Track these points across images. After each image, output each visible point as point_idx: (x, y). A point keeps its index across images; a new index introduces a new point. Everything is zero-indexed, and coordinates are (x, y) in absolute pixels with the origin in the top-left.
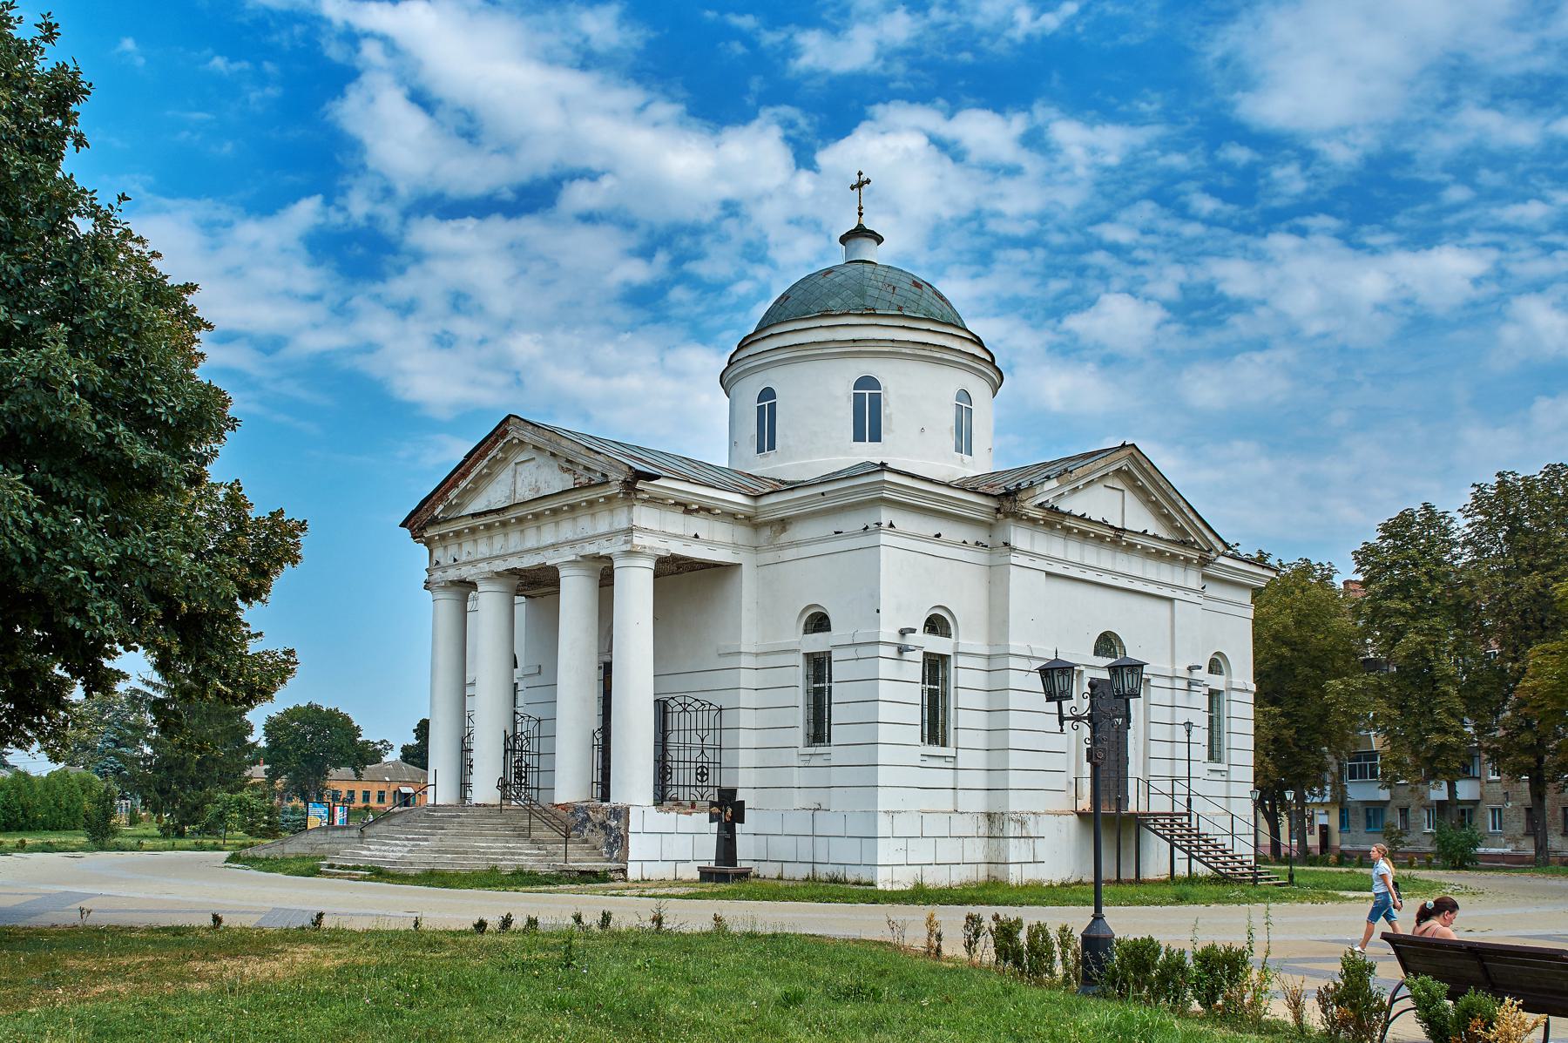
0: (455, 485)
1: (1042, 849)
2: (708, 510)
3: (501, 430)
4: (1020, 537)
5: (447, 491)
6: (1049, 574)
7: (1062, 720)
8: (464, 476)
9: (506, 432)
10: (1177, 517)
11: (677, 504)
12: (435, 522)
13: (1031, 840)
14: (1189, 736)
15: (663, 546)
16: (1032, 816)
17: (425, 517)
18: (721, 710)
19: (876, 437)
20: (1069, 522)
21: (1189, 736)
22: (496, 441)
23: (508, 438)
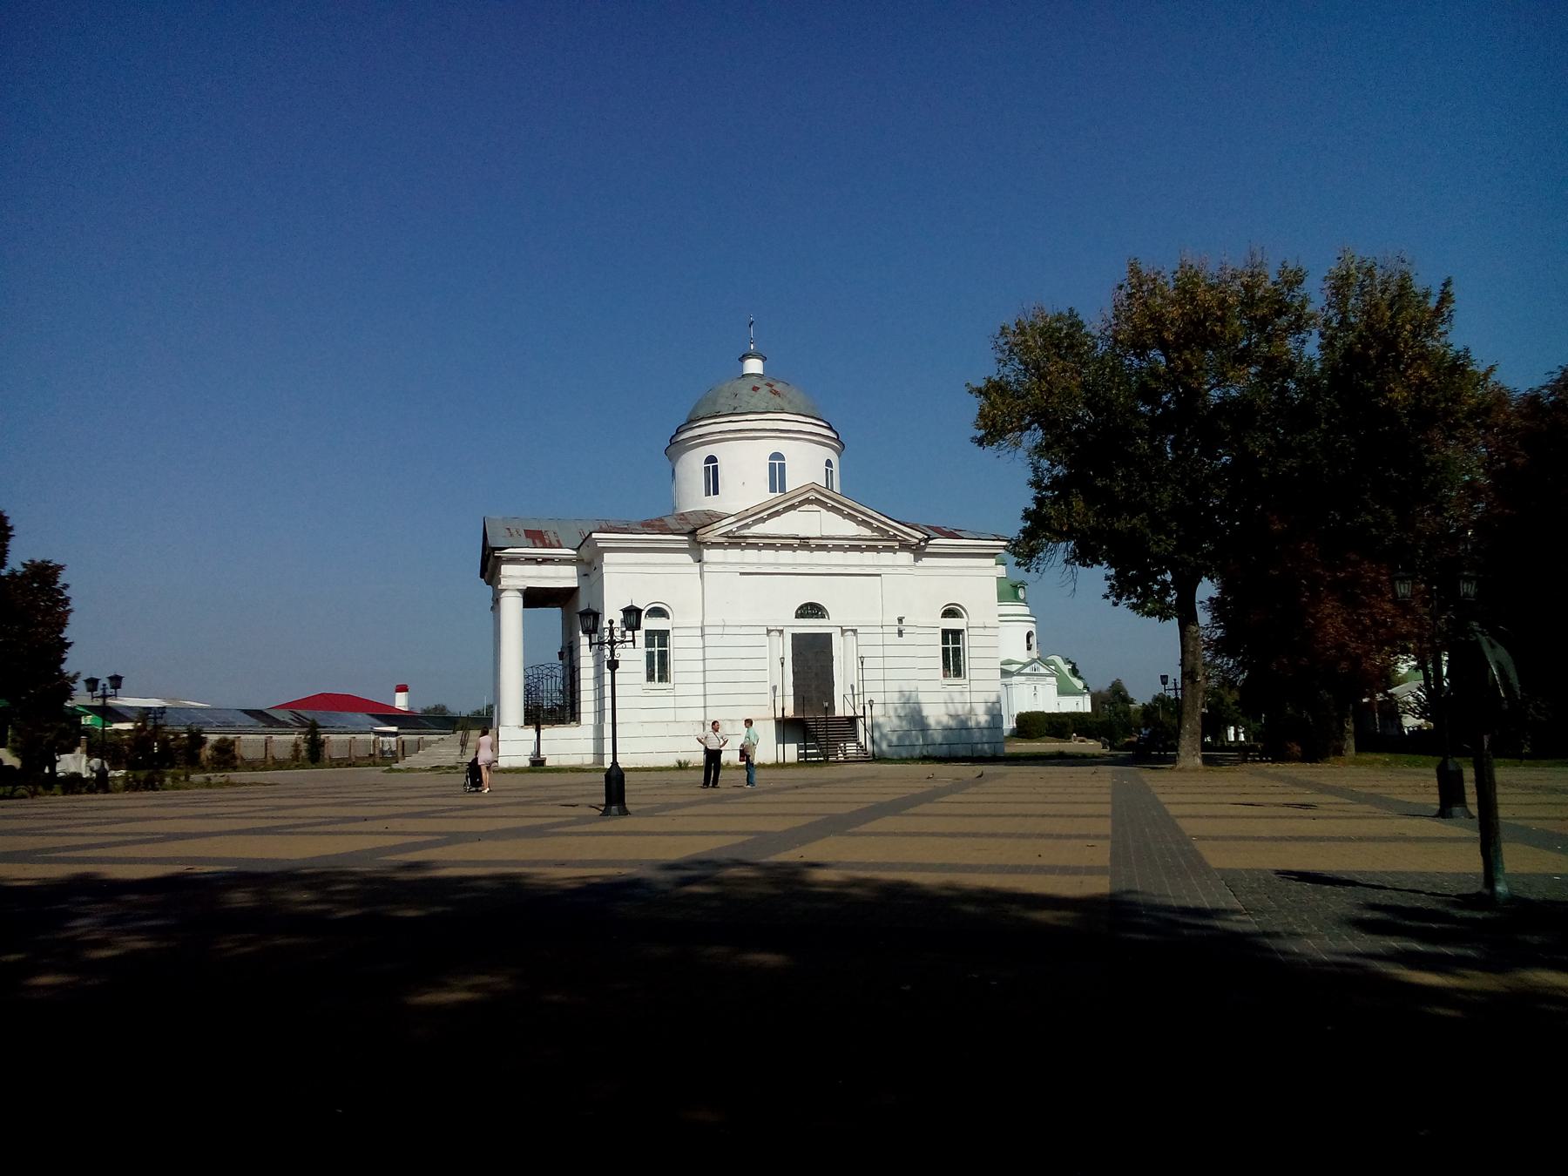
2: (553, 560)
4: (709, 555)
6: (741, 574)
7: (93, 698)
16: (729, 722)
19: (716, 492)
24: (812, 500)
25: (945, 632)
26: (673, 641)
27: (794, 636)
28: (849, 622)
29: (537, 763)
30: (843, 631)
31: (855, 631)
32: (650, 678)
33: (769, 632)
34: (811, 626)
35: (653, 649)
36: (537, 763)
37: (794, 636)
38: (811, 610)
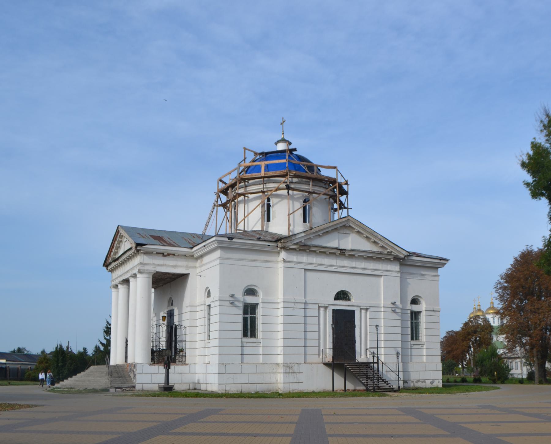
0: (111, 251)
1: (301, 378)
2: (174, 255)
3: (117, 231)
5: (110, 253)
8: (113, 247)
9: (119, 232)
10: (379, 242)
11: (158, 253)
12: (110, 263)
13: (295, 374)
14: (377, 331)
15: (154, 269)
16: (296, 365)
17: (108, 263)
18: (186, 327)
20: (312, 249)
21: (377, 331)
22: (117, 235)
23: (120, 233)
24: (347, 226)
25: (412, 312)
26: (260, 311)
27: (334, 311)
28: (364, 303)
29: (168, 389)
30: (361, 309)
31: (367, 309)
32: (245, 335)
33: (319, 307)
34: (342, 305)
35: (251, 316)
36: (168, 389)
37: (334, 311)
38: (342, 295)
